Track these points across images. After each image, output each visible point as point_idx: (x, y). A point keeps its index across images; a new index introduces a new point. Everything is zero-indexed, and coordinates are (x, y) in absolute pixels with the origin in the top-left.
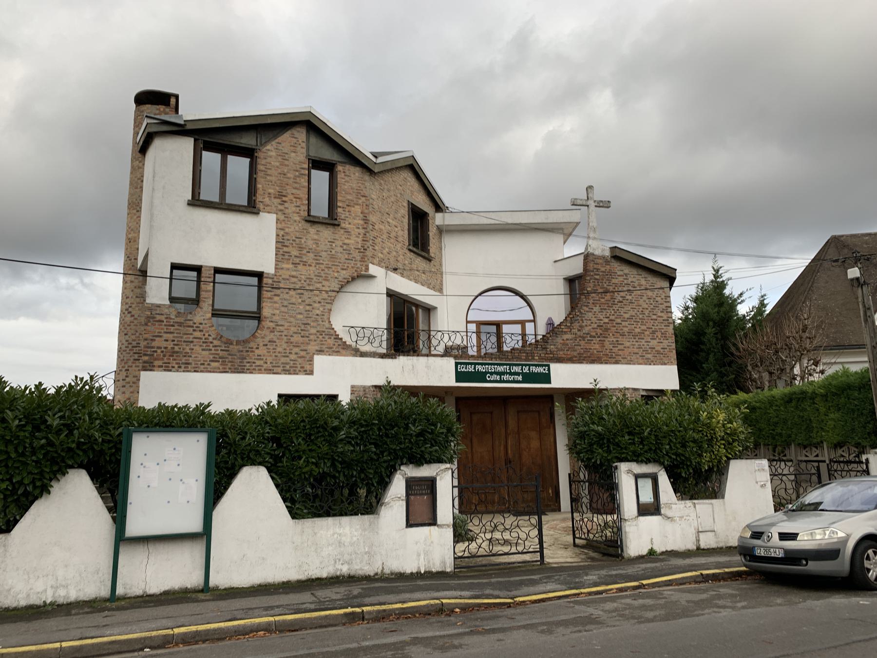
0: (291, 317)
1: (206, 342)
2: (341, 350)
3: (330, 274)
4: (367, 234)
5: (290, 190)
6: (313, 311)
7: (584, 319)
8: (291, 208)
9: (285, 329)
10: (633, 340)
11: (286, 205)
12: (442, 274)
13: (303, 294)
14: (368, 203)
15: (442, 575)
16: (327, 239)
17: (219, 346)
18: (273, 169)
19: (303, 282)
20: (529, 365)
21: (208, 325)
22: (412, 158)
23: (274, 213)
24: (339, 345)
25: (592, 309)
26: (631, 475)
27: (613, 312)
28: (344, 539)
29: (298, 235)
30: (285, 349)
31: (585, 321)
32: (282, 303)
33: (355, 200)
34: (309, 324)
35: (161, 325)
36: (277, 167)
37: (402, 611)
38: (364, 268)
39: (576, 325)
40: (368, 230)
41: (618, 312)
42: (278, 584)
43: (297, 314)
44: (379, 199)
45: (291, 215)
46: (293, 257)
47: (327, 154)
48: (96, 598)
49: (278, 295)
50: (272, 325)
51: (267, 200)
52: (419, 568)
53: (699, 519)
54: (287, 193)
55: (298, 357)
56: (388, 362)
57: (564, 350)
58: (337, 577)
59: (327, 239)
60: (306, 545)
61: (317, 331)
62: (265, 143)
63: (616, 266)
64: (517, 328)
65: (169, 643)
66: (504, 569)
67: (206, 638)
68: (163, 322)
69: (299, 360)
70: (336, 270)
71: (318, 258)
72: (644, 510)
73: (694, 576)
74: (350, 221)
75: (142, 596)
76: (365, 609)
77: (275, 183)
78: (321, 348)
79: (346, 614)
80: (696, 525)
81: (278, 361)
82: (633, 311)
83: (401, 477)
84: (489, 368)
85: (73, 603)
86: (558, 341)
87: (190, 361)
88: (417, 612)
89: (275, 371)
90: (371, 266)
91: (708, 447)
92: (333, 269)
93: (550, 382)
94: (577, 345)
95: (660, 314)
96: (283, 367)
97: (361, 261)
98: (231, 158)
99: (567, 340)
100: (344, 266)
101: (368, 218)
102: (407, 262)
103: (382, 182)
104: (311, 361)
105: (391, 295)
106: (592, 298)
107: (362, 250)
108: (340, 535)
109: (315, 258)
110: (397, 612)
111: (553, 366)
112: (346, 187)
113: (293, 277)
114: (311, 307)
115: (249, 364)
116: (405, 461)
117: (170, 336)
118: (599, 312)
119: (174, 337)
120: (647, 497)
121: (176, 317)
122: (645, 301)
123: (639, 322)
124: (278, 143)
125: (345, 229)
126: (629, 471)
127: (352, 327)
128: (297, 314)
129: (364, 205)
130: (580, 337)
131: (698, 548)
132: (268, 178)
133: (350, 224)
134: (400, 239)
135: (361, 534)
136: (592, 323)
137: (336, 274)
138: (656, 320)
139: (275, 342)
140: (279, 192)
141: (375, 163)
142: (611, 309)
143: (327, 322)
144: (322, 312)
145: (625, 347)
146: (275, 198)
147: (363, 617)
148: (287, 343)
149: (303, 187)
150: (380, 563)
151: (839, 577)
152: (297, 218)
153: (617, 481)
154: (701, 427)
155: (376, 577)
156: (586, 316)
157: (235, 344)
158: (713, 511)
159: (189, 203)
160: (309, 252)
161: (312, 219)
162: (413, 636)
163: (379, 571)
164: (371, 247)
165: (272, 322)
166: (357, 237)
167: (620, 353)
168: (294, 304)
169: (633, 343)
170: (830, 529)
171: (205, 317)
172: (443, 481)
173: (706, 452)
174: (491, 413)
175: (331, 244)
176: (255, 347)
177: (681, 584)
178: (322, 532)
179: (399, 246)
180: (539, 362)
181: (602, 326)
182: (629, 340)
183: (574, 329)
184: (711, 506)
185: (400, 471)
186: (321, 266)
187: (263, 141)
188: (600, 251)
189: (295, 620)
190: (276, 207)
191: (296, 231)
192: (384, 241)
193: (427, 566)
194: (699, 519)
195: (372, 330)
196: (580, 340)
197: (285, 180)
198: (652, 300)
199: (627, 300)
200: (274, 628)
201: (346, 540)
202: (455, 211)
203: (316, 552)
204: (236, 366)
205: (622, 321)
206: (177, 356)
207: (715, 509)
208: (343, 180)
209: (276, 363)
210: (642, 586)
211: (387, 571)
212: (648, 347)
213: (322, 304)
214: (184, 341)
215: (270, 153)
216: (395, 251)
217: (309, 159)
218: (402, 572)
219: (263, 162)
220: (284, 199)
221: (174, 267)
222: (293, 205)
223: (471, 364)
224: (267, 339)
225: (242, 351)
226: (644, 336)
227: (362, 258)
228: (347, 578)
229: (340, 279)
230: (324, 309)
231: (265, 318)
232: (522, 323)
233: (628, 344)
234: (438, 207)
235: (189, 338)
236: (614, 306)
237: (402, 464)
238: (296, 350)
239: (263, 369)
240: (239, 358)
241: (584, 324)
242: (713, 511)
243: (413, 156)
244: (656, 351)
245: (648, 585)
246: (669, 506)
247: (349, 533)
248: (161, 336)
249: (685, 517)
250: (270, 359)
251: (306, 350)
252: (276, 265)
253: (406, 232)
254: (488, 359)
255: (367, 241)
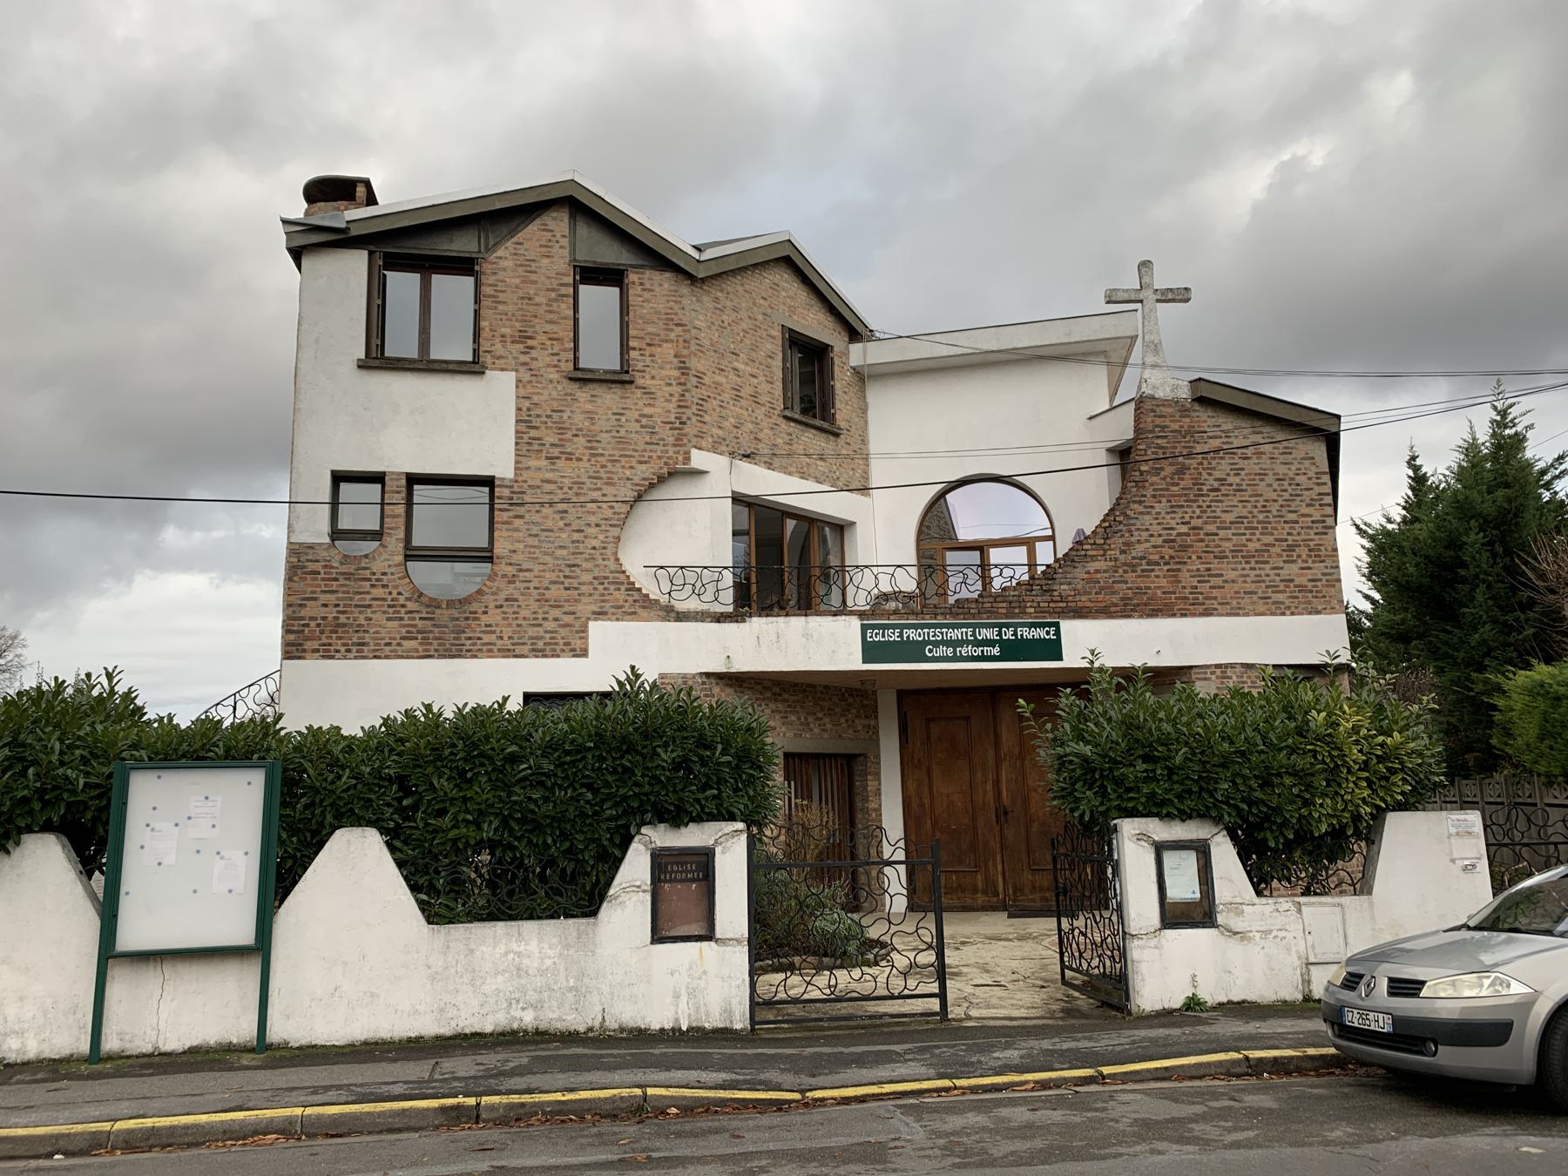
0: (546, 554)
1: (394, 606)
2: (639, 610)
3: (617, 473)
4: (687, 394)
5: (540, 326)
6: (587, 541)
7: (1133, 528)
8: (543, 358)
9: (535, 577)
10: (1243, 565)
11: (534, 353)
12: (866, 459)
13: (566, 512)
14: (687, 337)
15: (723, 1035)
16: (609, 409)
17: (417, 612)
18: (509, 290)
19: (566, 489)
20: (1016, 626)
21: (396, 576)
22: (787, 244)
23: (512, 370)
24: (635, 601)
25: (1152, 507)
26: (1145, 844)
27: (1198, 511)
28: (526, 961)
29: (555, 405)
30: (535, 613)
31: (1136, 533)
32: (528, 530)
33: (662, 333)
34: (578, 566)
35: (317, 579)
36: (517, 287)
37: (559, 1108)
38: (680, 458)
39: (1117, 541)
40: (689, 386)
41: (1209, 510)
42: (400, 1041)
43: (556, 548)
44: (713, 328)
45: (543, 370)
46: (547, 446)
47: (609, 253)
48: (72, 1055)
49: (522, 517)
50: (511, 570)
51: (498, 348)
52: (677, 1020)
53: (1309, 937)
54: (535, 332)
55: (561, 626)
56: (730, 628)
57: (1090, 593)
58: (514, 1033)
59: (609, 409)
60: (453, 971)
61: (595, 578)
62: (494, 245)
63: (1206, 419)
64: (1019, 554)
65: (100, 1146)
66: (856, 1028)
67: (170, 1141)
68: (319, 573)
69: (561, 630)
70: (627, 465)
71: (595, 444)
72: (1175, 916)
73: (1226, 1061)
74: (654, 372)
75: (151, 1055)
76: (485, 1100)
77: (513, 315)
78: (602, 607)
79: (443, 1110)
80: (1302, 949)
81: (522, 634)
82: (1244, 507)
83: (642, 847)
84: (931, 634)
85: (33, 1063)
86: (1078, 575)
87: (367, 640)
88: (589, 1110)
89: (517, 652)
90: (695, 453)
91: (1328, 785)
92: (623, 463)
93: (1060, 659)
94: (1119, 582)
95: (1304, 510)
96: (532, 644)
97: (675, 445)
98: (437, 279)
99: (1097, 571)
100: (644, 456)
101: (688, 365)
102: (779, 441)
103: (719, 294)
104: (583, 632)
105: (737, 499)
106: (1152, 484)
107: (677, 425)
108: (519, 954)
109: (590, 445)
110: (549, 1109)
111: (1067, 626)
112: (645, 311)
113: (548, 481)
114: (582, 534)
115: (470, 642)
116: (649, 816)
117: (332, 598)
118: (1168, 513)
119: (338, 599)
120: (1184, 886)
121: (342, 564)
122: (1270, 485)
123: (1257, 528)
124: (518, 243)
125: (645, 388)
126: (1142, 837)
127: (662, 567)
128: (556, 548)
129: (681, 342)
130: (1125, 564)
131: (1307, 999)
132: (500, 307)
133: (653, 378)
134: (763, 399)
135: (561, 954)
136: (1152, 536)
137: (628, 473)
138: (1297, 522)
139: (517, 600)
140: (520, 331)
141: (698, 261)
142: (1195, 505)
143: (612, 558)
144: (602, 542)
145: (1226, 581)
146: (513, 342)
147: (478, 1116)
148: (539, 601)
149: (565, 318)
150: (598, 1009)
151: (1512, 1085)
152: (555, 376)
153: (1116, 857)
154: (1312, 744)
155: (590, 1035)
156: (1138, 523)
157: (444, 606)
158: (1344, 921)
159: (360, 364)
160: (577, 435)
161: (579, 375)
162: (495, 1163)
163: (597, 1024)
164: (694, 419)
165: (511, 564)
166: (667, 401)
167: (1215, 593)
168: (552, 531)
169: (1245, 572)
170: (1493, 975)
171: (390, 563)
172: (728, 854)
173: (1324, 795)
174: (968, 719)
175: (618, 417)
176: (480, 611)
177: (1192, 1078)
178: (484, 948)
179: (760, 412)
180: (1036, 617)
181: (1173, 541)
182: (1234, 566)
183: (1110, 549)
184: (1338, 909)
185: (641, 837)
186: (599, 459)
187: (492, 242)
188: (1168, 389)
189: (342, 1115)
190: (515, 358)
191: (553, 399)
192: (725, 404)
193: (693, 1018)
194: (1309, 938)
195: (699, 570)
196: (1125, 572)
197: (531, 308)
198: (1286, 483)
199: (1231, 485)
200: (299, 1129)
201: (532, 964)
202: (886, 336)
203: (473, 986)
204: (448, 646)
205: (1218, 528)
206: (343, 632)
207: (1347, 917)
208: (640, 299)
209: (518, 638)
210: (1100, 1079)
211: (612, 1024)
212: (1278, 579)
213: (603, 527)
214: (357, 606)
215: (504, 263)
216: (752, 422)
217: (575, 266)
218: (643, 1027)
219: (491, 280)
220: (530, 342)
221: (339, 478)
222: (547, 352)
223: (894, 627)
224: (502, 596)
225: (457, 619)
226: (1270, 556)
227: (677, 440)
228: (534, 1034)
229: (636, 480)
230: (607, 537)
231: (498, 558)
232: (1029, 543)
233: (1232, 575)
234: (854, 331)
235: (365, 599)
236: (1201, 499)
237: (644, 824)
238: (556, 613)
239: (495, 648)
240: (453, 632)
241: (1133, 539)
242: (1344, 921)
243: (789, 241)
244: (1296, 586)
245: (1113, 1076)
246: (1236, 908)
247: (536, 951)
248: (315, 599)
249: (1274, 933)
250: (507, 632)
251: (574, 613)
252: (517, 462)
253: (779, 385)
254: (927, 617)
255: (686, 407)
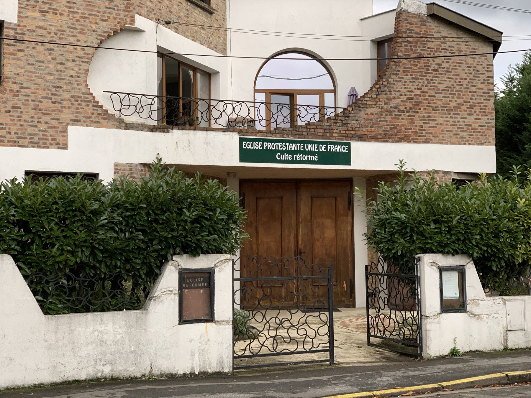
0: (39, 77)
3: (87, 26)
6: (66, 71)
7: (392, 90)
9: (32, 93)
10: (447, 115)
13: (53, 50)
15: (219, 375)
19: (53, 34)
20: (327, 143)
24: (99, 114)
25: (402, 78)
27: (426, 82)
28: (105, 336)
30: (32, 117)
31: (393, 93)
32: (27, 60)
34: (61, 87)
38: (128, 20)
39: (383, 97)
41: (432, 82)
42: (29, 387)
43: (46, 74)
49: (23, 51)
50: (16, 87)
52: (193, 368)
53: (508, 317)
57: (367, 127)
58: (98, 379)
60: (61, 343)
61: (72, 97)
63: (434, 27)
64: (315, 100)
66: (290, 369)
70: (94, 21)
78: (76, 117)
80: (505, 323)
81: (24, 131)
82: (450, 81)
83: (173, 268)
84: (280, 146)
89: (20, 144)
91: (524, 238)
92: (91, 20)
93: (349, 163)
94: (383, 121)
95: (480, 86)
96: (31, 138)
97: (125, 11)
99: (372, 114)
100: (104, 16)
102: (182, 14)
104: (64, 132)
105: (162, 54)
106: (403, 64)
108: (101, 332)
113: (41, 28)
114: (63, 66)
116: (178, 250)
118: (410, 82)
122: (463, 70)
123: (455, 94)
126: (434, 264)
127: (115, 93)
128: (46, 74)
130: (387, 111)
136: (401, 95)
137: (94, 27)
138: (475, 92)
139: (20, 108)
142: (425, 78)
143: (84, 84)
144: (77, 73)
145: (437, 124)
148: (35, 109)
150: (148, 363)
153: (419, 275)
154: (517, 216)
155: (143, 379)
163: (147, 373)
165: (15, 83)
168: (43, 62)
169: (447, 119)
173: (521, 243)
174: (281, 198)
177: (484, 386)
178: (80, 329)
180: (338, 139)
181: (412, 99)
182: (442, 115)
183: (379, 101)
185: (172, 262)
186: (75, 15)
188: (415, 7)
194: (508, 317)
195: (139, 97)
196: (386, 115)
198: (471, 69)
199: (444, 68)
203: (73, 352)
205: (436, 93)
207: (526, 306)
209: (21, 134)
210: (443, 388)
211: (156, 372)
212: (464, 124)
213: (77, 63)
218: (174, 373)
223: (259, 140)
224: (10, 104)
226: (461, 111)
227: (126, 7)
230: (80, 70)
231: (7, 78)
232: (321, 93)
233: (440, 120)
236: (428, 75)
237: (175, 254)
239: (6, 140)
241: (392, 96)
244: (472, 129)
245: (447, 387)
246: (476, 302)
249: (493, 315)
250: (13, 129)
251: (58, 119)
254: (278, 135)
